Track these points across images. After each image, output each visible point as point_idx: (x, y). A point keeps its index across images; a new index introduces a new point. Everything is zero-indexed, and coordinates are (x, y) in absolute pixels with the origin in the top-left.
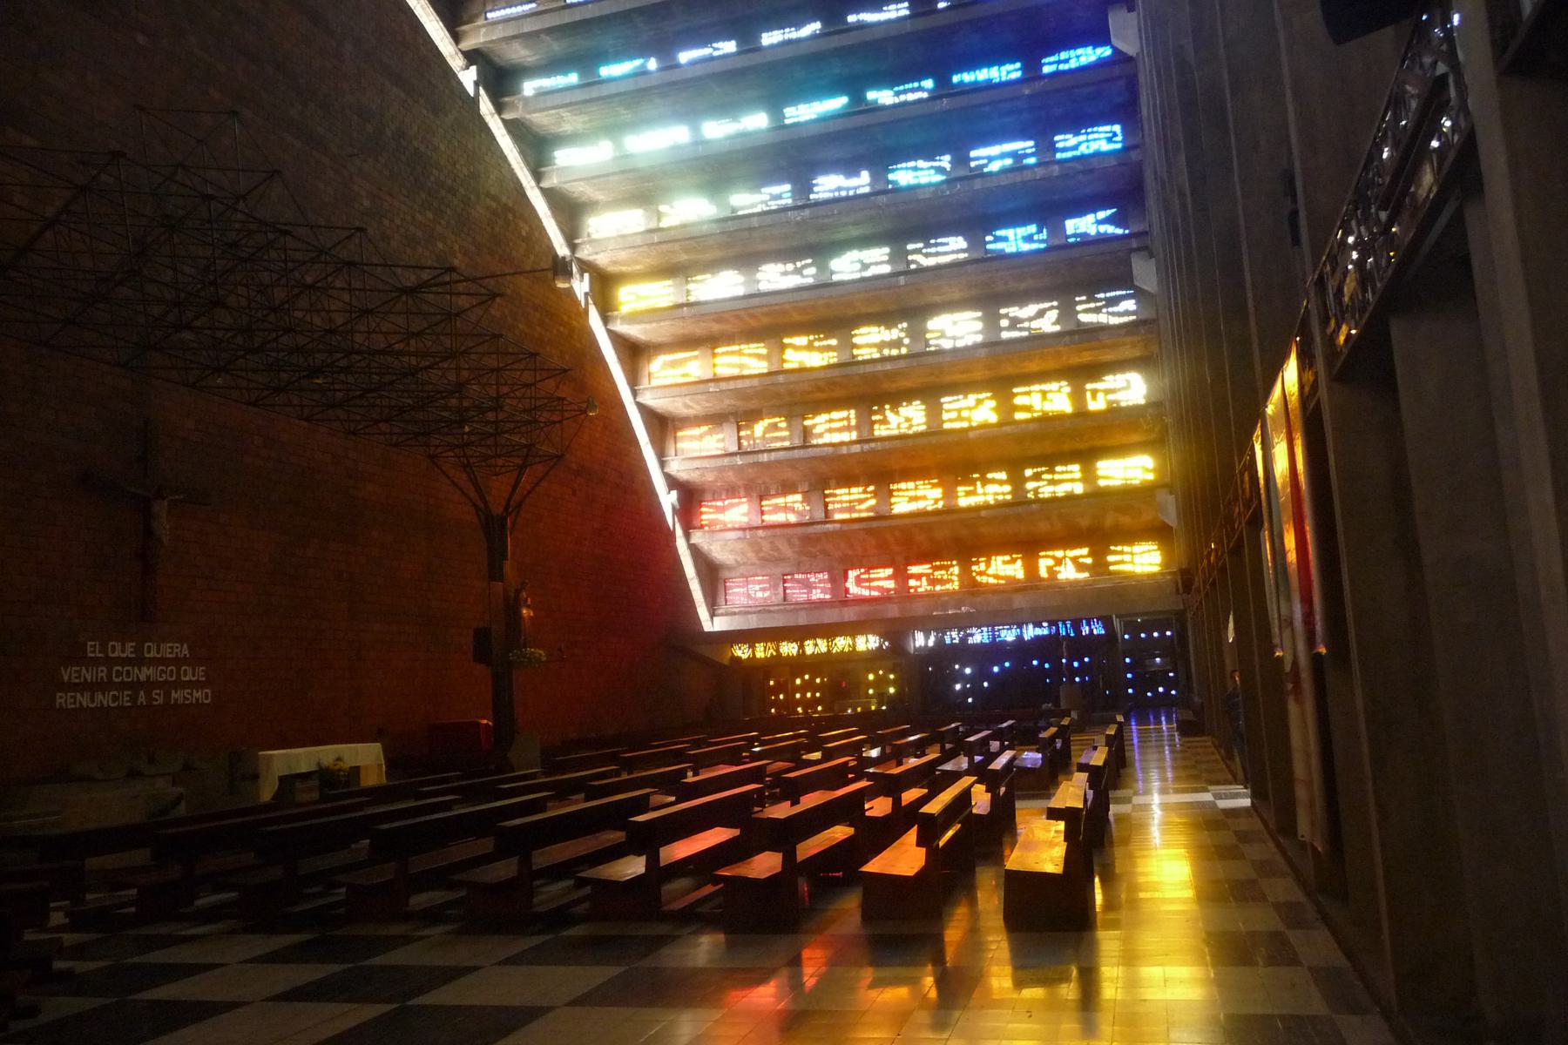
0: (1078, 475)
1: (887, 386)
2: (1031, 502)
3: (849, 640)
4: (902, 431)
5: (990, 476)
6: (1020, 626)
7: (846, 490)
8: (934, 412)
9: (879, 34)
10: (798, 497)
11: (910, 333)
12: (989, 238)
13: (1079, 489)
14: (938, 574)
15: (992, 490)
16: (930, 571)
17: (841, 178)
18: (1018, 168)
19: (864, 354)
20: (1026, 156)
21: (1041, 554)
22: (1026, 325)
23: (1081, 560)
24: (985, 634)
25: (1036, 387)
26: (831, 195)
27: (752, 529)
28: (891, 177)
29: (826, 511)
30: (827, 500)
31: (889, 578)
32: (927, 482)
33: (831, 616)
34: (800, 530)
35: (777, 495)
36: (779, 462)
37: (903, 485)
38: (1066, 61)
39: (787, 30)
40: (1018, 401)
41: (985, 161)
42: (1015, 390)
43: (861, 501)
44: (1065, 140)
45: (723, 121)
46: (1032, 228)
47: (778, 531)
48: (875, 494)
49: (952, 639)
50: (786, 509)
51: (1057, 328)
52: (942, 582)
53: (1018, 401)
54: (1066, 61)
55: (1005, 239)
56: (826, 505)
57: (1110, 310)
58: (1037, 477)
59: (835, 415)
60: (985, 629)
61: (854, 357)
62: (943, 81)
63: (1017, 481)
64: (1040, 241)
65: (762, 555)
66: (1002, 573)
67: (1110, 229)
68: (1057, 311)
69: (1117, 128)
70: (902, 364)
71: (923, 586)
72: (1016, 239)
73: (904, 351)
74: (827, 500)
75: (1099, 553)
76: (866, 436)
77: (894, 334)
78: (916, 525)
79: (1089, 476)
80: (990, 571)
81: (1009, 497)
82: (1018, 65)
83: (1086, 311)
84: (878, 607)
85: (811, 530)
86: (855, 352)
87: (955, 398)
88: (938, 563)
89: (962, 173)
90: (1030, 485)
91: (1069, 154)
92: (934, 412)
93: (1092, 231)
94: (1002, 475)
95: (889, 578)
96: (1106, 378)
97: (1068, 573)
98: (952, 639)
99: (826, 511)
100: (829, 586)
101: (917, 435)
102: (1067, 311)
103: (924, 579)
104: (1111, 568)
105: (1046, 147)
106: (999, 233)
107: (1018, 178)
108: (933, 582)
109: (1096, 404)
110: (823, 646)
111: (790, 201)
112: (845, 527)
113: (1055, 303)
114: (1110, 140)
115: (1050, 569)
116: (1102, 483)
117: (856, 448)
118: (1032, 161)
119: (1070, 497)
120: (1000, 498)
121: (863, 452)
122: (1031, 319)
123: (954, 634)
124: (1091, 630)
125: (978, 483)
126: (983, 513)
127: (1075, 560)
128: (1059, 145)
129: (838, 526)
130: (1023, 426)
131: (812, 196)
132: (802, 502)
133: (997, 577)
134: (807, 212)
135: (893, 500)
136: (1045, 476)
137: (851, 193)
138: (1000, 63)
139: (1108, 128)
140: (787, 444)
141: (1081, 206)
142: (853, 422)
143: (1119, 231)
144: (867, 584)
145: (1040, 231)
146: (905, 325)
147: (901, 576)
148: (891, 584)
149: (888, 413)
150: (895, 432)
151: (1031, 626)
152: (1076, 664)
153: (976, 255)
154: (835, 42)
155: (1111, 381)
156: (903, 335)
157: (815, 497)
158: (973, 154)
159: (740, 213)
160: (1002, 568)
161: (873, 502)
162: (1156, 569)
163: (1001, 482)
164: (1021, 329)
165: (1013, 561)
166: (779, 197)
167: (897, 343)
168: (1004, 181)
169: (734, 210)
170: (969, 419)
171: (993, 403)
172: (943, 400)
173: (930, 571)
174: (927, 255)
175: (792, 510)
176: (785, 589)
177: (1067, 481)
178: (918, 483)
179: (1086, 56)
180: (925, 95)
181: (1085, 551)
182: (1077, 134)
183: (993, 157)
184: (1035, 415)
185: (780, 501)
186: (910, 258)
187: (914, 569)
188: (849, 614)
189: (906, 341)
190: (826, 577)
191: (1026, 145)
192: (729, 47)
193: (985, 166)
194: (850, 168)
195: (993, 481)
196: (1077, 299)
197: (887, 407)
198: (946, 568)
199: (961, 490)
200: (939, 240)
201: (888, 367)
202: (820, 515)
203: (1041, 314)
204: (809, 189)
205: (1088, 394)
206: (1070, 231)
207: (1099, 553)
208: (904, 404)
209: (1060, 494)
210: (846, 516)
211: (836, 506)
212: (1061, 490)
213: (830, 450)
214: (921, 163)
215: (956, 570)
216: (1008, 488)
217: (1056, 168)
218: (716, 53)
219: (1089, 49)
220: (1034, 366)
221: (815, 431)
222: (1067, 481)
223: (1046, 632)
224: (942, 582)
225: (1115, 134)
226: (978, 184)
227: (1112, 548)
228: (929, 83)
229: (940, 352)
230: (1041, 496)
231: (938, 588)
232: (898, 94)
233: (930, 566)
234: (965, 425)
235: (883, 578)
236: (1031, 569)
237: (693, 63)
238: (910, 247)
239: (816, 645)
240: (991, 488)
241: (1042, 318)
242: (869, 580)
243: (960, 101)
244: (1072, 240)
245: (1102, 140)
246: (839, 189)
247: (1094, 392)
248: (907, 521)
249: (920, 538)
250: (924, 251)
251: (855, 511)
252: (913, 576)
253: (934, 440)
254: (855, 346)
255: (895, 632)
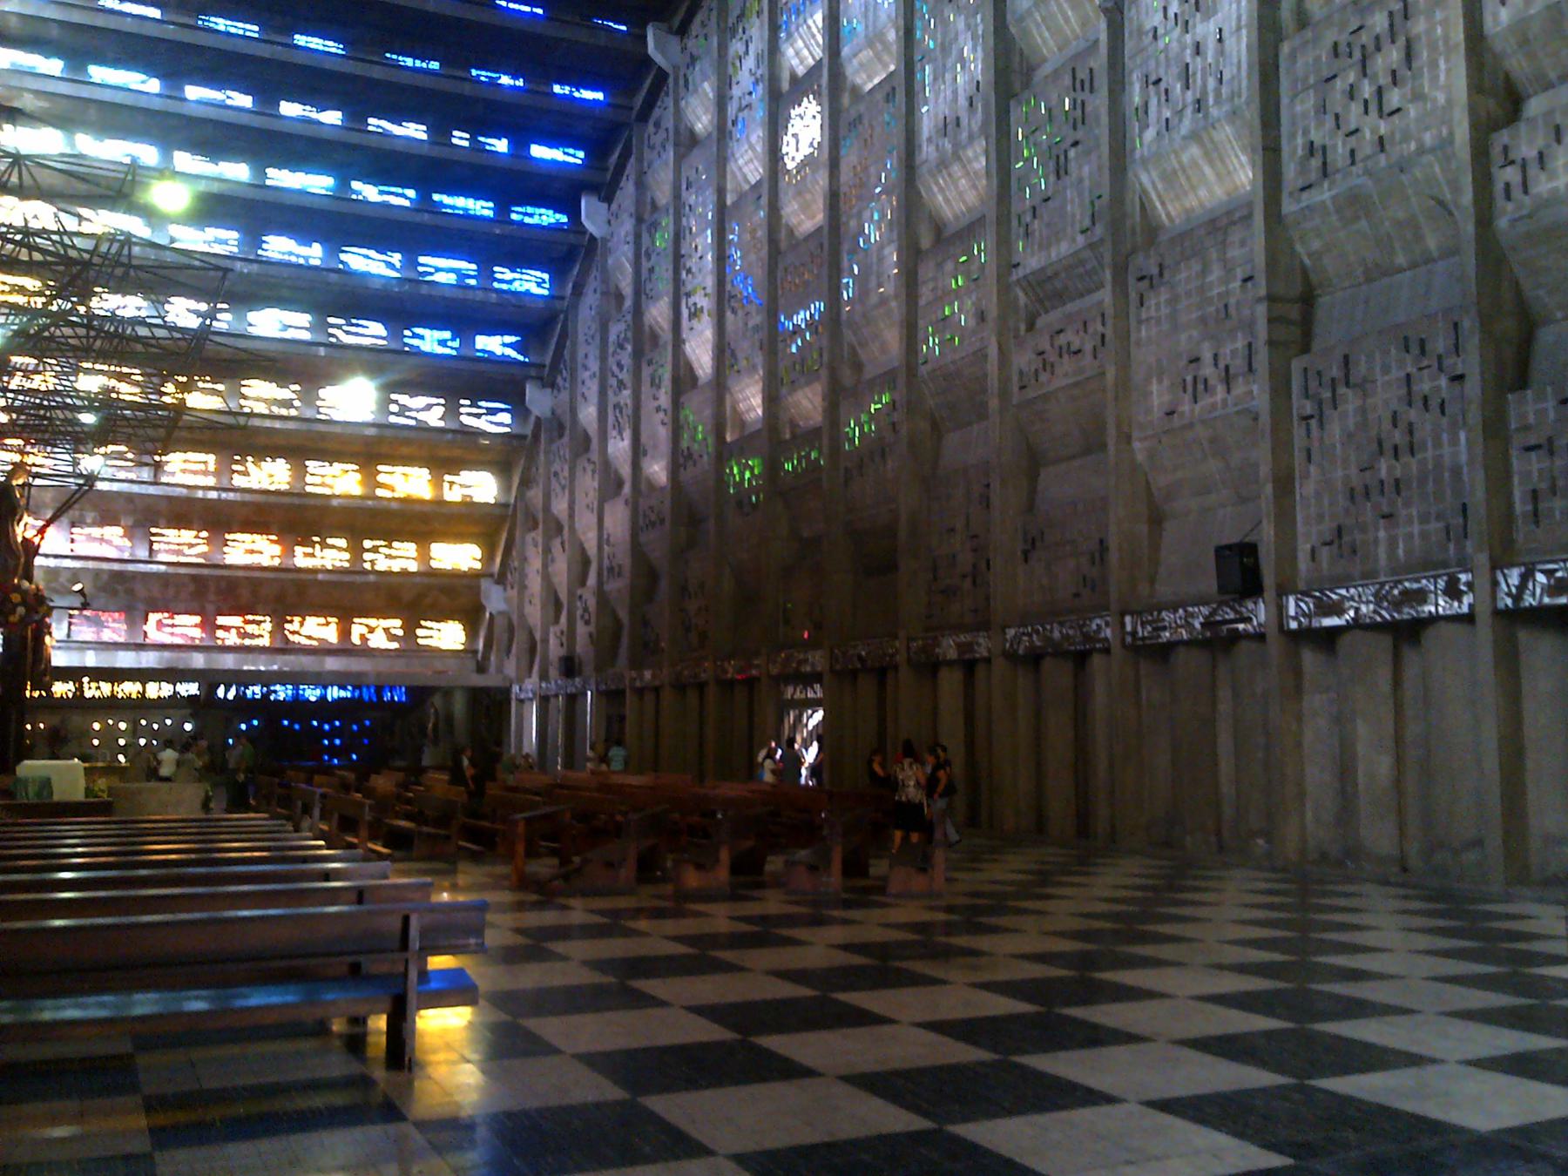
0: (415, 554)
1: (262, 440)
2: (366, 572)
3: (138, 686)
4: (266, 486)
5: (329, 541)
6: (325, 688)
7: (175, 532)
8: (300, 472)
9: (399, 146)
10: (119, 531)
11: (302, 396)
12: (407, 333)
13: (413, 567)
14: (250, 629)
15: (330, 556)
16: (242, 625)
17: (292, 242)
18: (461, 286)
19: (250, 406)
20: (470, 277)
21: (356, 620)
22: (413, 414)
23: (393, 631)
24: (290, 692)
25: (399, 469)
26: (280, 257)
27: (56, 556)
28: (343, 257)
29: (151, 550)
30: (153, 539)
31: (196, 626)
32: (265, 537)
33: (125, 660)
34: (116, 567)
35: (94, 524)
36: (118, 494)
37: (238, 536)
38: (531, 215)
39: (308, 108)
40: (381, 478)
41: (432, 270)
42: (380, 468)
43: (191, 546)
44: (503, 273)
45: (199, 157)
46: (447, 335)
47: (91, 565)
48: (209, 541)
49: (254, 693)
50: (102, 540)
51: (441, 424)
52: (253, 636)
53: (381, 478)
54: (531, 215)
55: (422, 337)
56: (151, 543)
57: (490, 418)
58: (375, 550)
59: (191, 456)
60: (290, 687)
61: (242, 407)
62: (425, 196)
63: (356, 551)
64: (452, 348)
65: (53, 585)
66: (315, 636)
67: (513, 354)
68: (443, 409)
69: (546, 276)
70: (291, 425)
71: (232, 639)
72: (431, 341)
73: (293, 412)
74: (153, 539)
75: (411, 627)
76: (225, 484)
77: (285, 394)
78: (247, 578)
79: (424, 556)
80: (304, 631)
81: (347, 565)
82: (491, 204)
83: (469, 414)
84: (183, 655)
85: (131, 567)
86: (242, 402)
87: (321, 463)
88: (250, 617)
89: (412, 275)
90: (367, 556)
91: (505, 287)
92: (300, 472)
93: (499, 351)
94: (342, 543)
95: (196, 626)
96: (462, 473)
97: (378, 641)
98: (254, 693)
99: (151, 550)
100: (125, 627)
101: (278, 493)
102: (452, 411)
103: (234, 631)
104: (420, 641)
105: (486, 273)
106: (418, 330)
107: (459, 294)
108: (244, 635)
109: (453, 495)
110: (106, 688)
111: (235, 250)
112: (171, 570)
113: (442, 401)
114: (539, 285)
115: (363, 637)
116: (434, 564)
117: (213, 495)
118: (473, 282)
119: (404, 573)
120: (338, 564)
121: (219, 500)
122: (418, 411)
123: (257, 689)
124: (392, 697)
125: (317, 546)
126: (320, 577)
127: (386, 630)
128: (498, 276)
129: (163, 568)
130: (385, 503)
131: (260, 252)
132: (125, 536)
133: (309, 637)
134: (255, 268)
135: (226, 549)
136: (381, 549)
137: (301, 261)
138: (477, 199)
139: (538, 274)
140: (132, 476)
141: (490, 331)
142: (212, 467)
143: (521, 358)
144: (169, 630)
145: (453, 339)
146: (297, 387)
147: (209, 626)
148: (197, 633)
149: (250, 465)
150: (256, 486)
151: (336, 688)
152: (327, 727)
153: (394, 346)
154: (354, 138)
155: (466, 476)
156: (294, 396)
157: (139, 532)
158: (422, 259)
159: (175, 245)
160: (316, 629)
161: (205, 548)
162: (462, 647)
163: (340, 549)
164: (408, 417)
165: (328, 624)
166: (226, 242)
167: (287, 404)
168: (448, 293)
169: (173, 240)
170: (331, 487)
171: (358, 476)
172: (307, 463)
173: (242, 625)
174: (347, 333)
175: (109, 542)
176: (70, 624)
177: (399, 558)
178: (256, 537)
179: (546, 217)
180: (407, 203)
181: (398, 623)
182: (513, 271)
183: (444, 270)
184: (396, 495)
185: (96, 532)
186: (331, 330)
187: (221, 620)
188: (148, 660)
189: (297, 403)
190: (123, 617)
191: (469, 267)
192: (245, 101)
193: (431, 274)
194: (305, 238)
195: (333, 547)
196: (462, 402)
197: (250, 459)
198: (259, 623)
199: (299, 550)
200: (361, 322)
201: (277, 425)
202: (143, 553)
203: (429, 407)
204: (259, 244)
205: (446, 485)
206: (478, 346)
207: (411, 627)
208: (268, 459)
209: (396, 569)
210: (174, 559)
211: (163, 546)
212: (396, 566)
213: (184, 491)
214: (372, 253)
215: (268, 626)
216: (347, 556)
217: (494, 295)
218: (229, 102)
219: (551, 212)
220: (405, 450)
221: (166, 468)
222: (399, 558)
223: (349, 695)
224: (253, 636)
225: (544, 281)
226: (424, 290)
227: (423, 623)
228: (411, 193)
229: (330, 422)
230: (377, 568)
231: (247, 642)
232: (382, 192)
233: (241, 619)
234: (327, 491)
235: (187, 627)
236: (345, 633)
237: (199, 102)
238: (331, 320)
239: (98, 688)
240: (327, 551)
241: (429, 411)
242: (173, 626)
243: (438, 220)
244: (479, 354)
245: (530, 283)
246: (291, 254)
247: (451, 483)
248: (241, 573)
249: (245, 594)
250: (345, 328)
251: (184, 555)
252: (221, 627)
253: (296, 501)
254: (245, 397)
255: (209, 679)
